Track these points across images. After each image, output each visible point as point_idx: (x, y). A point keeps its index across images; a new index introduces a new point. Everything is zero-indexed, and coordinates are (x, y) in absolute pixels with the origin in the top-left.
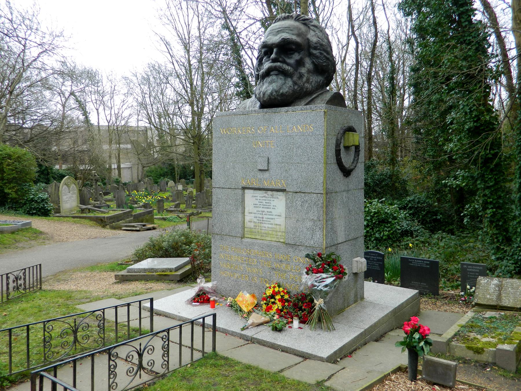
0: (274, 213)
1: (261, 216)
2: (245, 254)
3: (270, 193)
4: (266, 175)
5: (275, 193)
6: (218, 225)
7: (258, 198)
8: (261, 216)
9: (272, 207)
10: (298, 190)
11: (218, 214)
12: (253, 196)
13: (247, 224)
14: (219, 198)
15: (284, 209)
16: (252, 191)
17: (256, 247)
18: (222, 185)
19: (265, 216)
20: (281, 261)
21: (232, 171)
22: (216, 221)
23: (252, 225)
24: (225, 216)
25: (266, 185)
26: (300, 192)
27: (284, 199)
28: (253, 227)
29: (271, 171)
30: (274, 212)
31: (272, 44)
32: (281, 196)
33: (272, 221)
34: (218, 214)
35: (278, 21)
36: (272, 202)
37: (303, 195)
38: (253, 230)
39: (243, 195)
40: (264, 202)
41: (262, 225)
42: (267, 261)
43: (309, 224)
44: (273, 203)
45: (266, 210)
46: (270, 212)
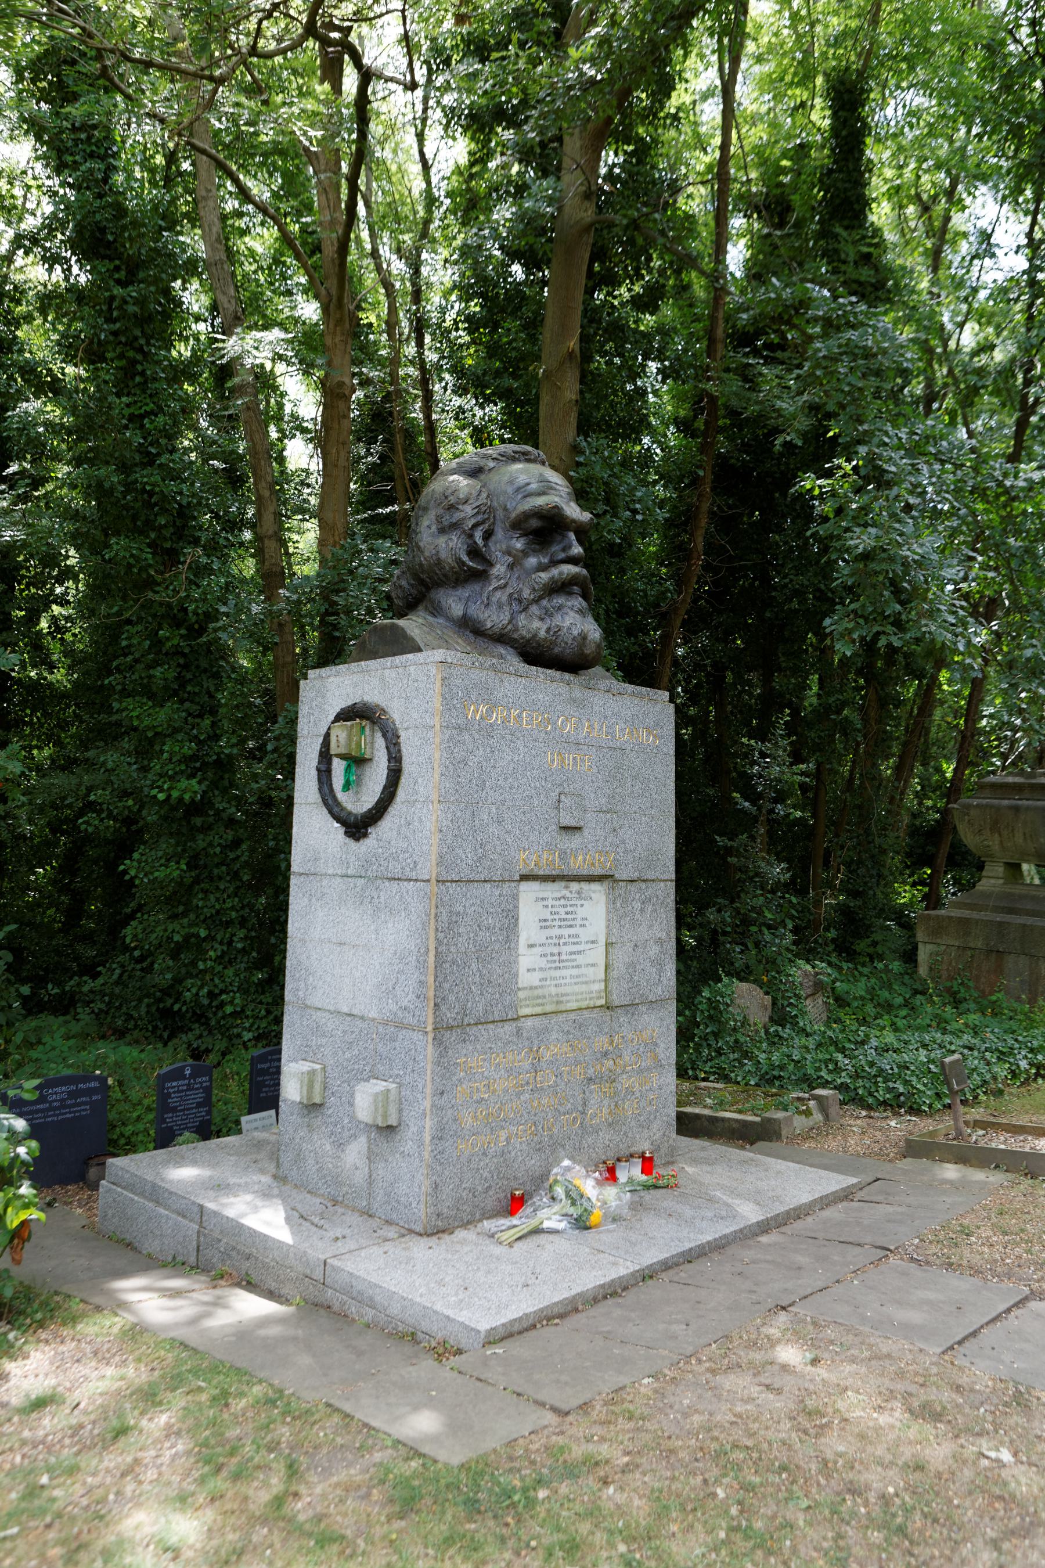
0: (583, 939)
1: (555, 950)
2: (526, 1065)
3: (575, 886)
4: (574, 842)
5: (584, 886)
6: (452, 998)
7: (550, 902)
8: (555, 950)
9: (579, 922)
10: (635, 876)
11: (454, 962)
12: (538, 900)
13: (526, 979)
14: (458, 914)
15: (603, 924)
16: (534, 886)
17: (554, 1035)
18: (465, 873)
19: (565, 949)
20: (606, 1054)
21: (493, 829)
22: (446, 986)
23: (534, 979)
24: (474, 967)
25: (578, 865)
26: (639, 880)
27: (603, 899)
28: (537, 983)
29: (586, 832)
30: (585, 935)
31: (574, 521)
32: (597, 892)
33: (581, 959)
34: (454, 962)
35: (529, 461)
36: (579, 910)
37: (643, 885)
38: (540, 992)
39: (516, 897)
40: (562, 910)
41: (558, 973)
42: (577, 1063)
43: (654, 950)
44: (581, 912)
45: (566, 932)
46: (576, 936)
